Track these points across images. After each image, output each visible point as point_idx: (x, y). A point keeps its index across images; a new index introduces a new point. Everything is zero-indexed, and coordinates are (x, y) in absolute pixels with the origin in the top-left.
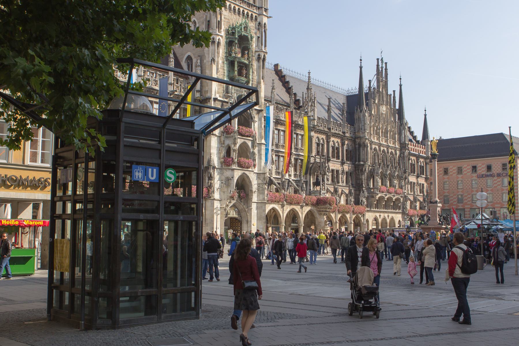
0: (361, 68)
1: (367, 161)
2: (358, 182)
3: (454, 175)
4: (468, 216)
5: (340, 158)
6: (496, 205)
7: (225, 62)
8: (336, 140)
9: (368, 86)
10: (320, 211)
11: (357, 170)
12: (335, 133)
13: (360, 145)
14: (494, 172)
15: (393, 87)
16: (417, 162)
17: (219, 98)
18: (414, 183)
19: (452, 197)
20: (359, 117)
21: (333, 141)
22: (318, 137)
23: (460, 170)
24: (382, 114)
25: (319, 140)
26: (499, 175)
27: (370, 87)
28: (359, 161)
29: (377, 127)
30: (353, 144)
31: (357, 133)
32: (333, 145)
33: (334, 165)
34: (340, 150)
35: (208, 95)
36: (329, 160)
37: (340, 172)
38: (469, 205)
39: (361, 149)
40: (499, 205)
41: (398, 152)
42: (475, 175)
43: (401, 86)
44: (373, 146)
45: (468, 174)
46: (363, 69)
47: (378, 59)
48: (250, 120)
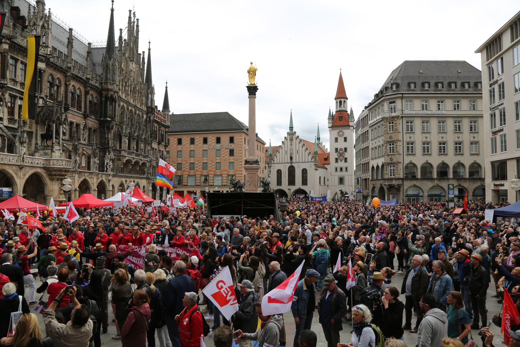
0: (112, 10)
1: (115, 117)
2: (103, 142)
4: (199, 181)
5: (83, 110)
6: (224, 173)
8: (77, 85)
9: (119, 35)
11: (104, 126)
13: (107, 98)
15: (142, 48)
16: (159, 130)
18: (156, 149)
19: (184, 164)
20: (107, 66)
21: (73, 86)
22: (51, 75)
23: (192, 141)
24: (131, 70)
25: (53, 78)
27: (121, 38)
28: (106, 116)
29: (126, 84)
31: (103, 84)
32: (73, 91)
33: (74, 117)
34: (83, 100)
36: (67, 109)
37: (82, 127)
38: (200, 171)
39: (108, 102)
40: (226, 173)
41: (145, 116)
43: (149, 50)
46: (114, 12)
47: (130, 11)
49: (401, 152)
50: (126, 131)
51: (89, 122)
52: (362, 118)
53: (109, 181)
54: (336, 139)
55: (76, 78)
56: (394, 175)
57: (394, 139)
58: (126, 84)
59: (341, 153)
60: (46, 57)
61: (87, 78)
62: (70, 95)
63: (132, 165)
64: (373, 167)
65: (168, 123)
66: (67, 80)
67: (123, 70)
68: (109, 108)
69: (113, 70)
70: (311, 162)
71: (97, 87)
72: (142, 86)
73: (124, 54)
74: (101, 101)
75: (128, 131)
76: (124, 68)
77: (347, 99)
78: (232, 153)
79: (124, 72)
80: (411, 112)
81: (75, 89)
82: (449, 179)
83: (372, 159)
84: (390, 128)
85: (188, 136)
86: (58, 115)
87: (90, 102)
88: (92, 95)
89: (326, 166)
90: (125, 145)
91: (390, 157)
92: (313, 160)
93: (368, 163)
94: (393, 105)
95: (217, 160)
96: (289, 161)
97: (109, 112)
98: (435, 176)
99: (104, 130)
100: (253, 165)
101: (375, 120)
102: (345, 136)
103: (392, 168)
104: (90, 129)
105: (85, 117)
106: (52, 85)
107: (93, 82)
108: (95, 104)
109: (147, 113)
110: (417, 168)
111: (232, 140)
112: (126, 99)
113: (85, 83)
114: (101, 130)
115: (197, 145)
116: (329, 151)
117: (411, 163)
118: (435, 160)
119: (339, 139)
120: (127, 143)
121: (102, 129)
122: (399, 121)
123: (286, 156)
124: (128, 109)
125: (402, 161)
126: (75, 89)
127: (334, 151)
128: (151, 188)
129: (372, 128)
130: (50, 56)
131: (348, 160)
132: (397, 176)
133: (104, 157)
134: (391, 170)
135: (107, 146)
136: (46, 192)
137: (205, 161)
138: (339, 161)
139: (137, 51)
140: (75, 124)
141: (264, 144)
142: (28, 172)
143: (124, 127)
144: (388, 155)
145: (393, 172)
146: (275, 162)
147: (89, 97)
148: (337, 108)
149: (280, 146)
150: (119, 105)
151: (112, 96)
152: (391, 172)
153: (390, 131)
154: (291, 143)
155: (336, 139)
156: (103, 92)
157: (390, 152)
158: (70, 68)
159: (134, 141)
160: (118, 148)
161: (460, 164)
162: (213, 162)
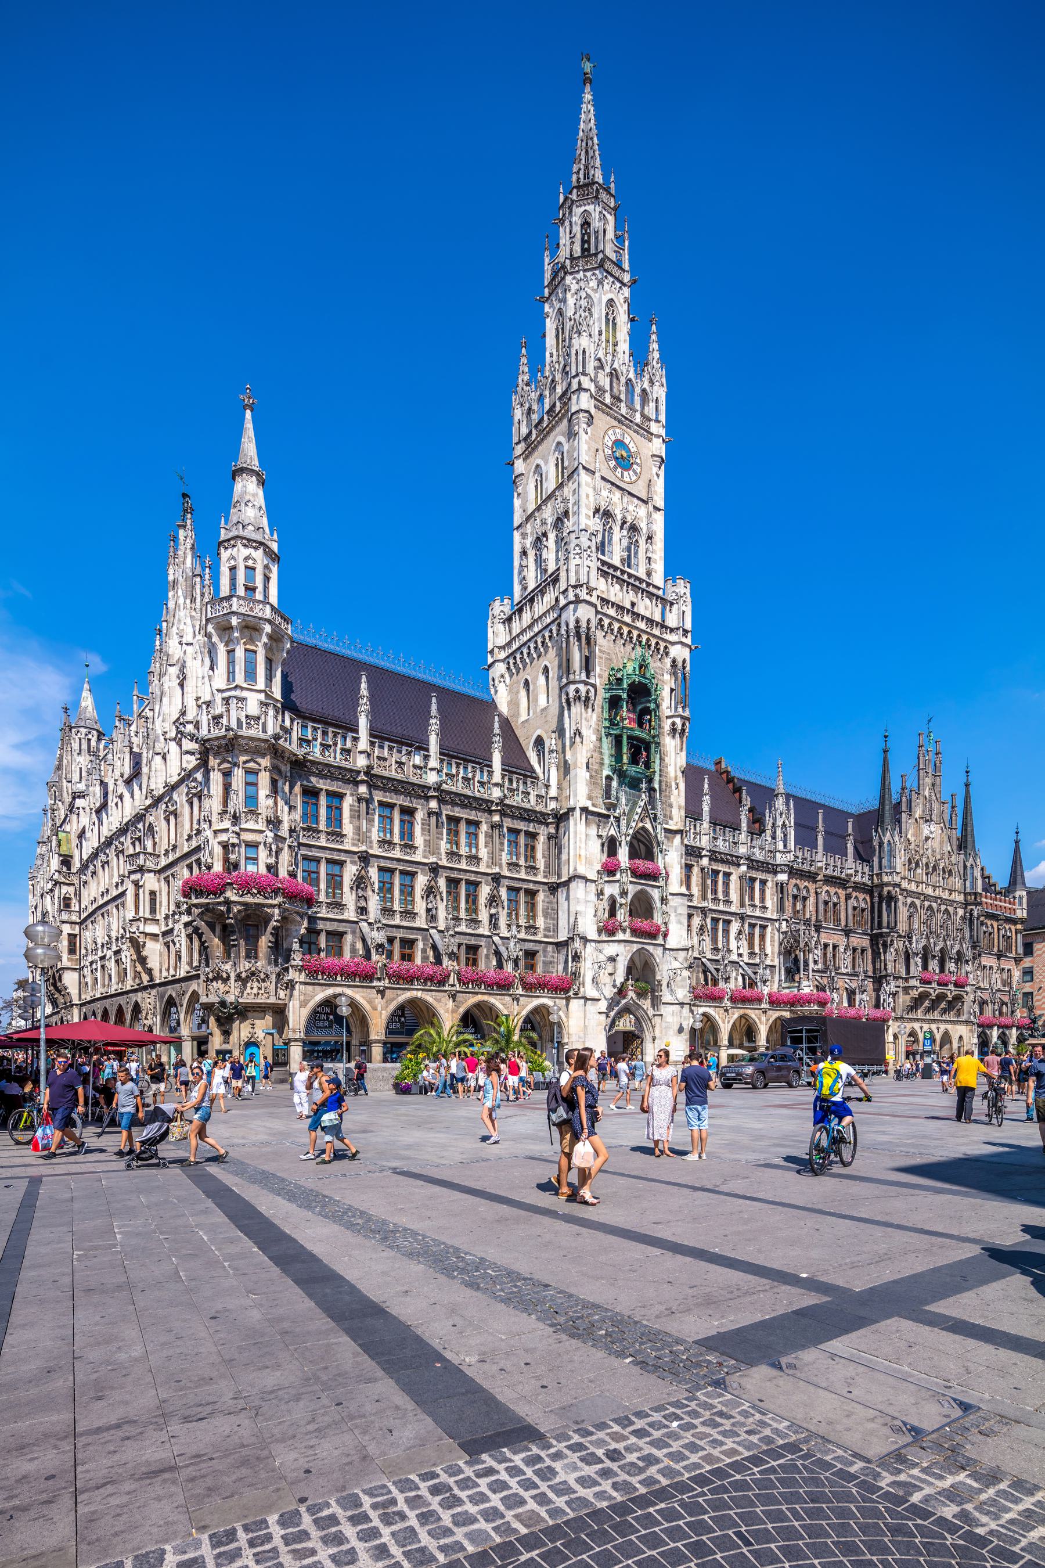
5: (843, 923)
7: (604, 739)
12: (832, 877)
17: (591, 808)
21: (827, 892)
22: (796, 885)
25: (798, 889)
34: (843, 908)
35: (572, 804)
36: (818, 929)
41: (961, 912)
44: (909, 900)
48: (656, 849)
55: (830, 880)
62: (821, 907)
65: (1022, 913)
74: (872, 904)
87: (855, 908)
108: (863, 910)
112: (919, 890)
151: (889, 892)
158: (820, 868)
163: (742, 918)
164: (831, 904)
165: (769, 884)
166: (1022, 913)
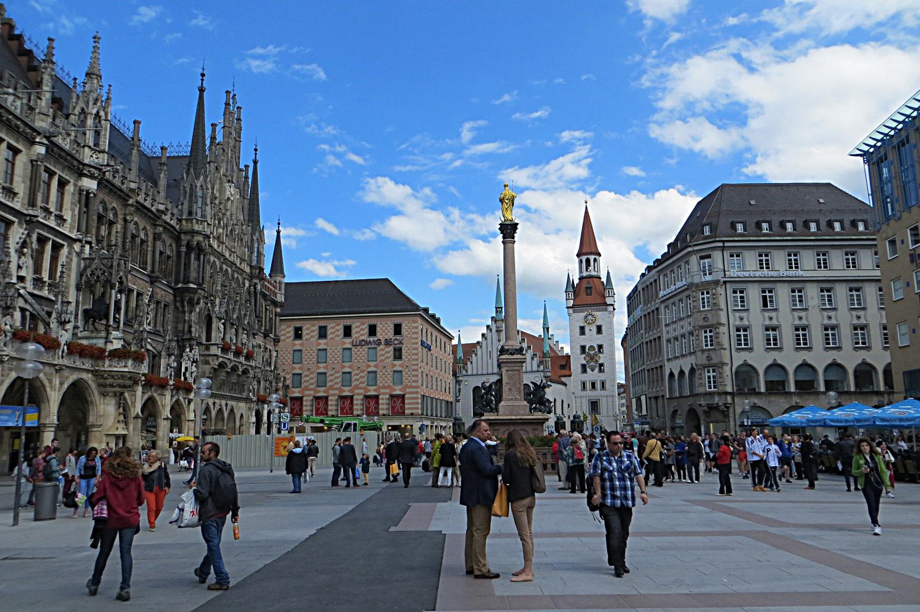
0: (202, 90)
3: (314, 339)
5: (149, 268)
6: (382, 391)
10: (104, 386)
11: (183, 298)
13: (189, 246)
14: (381, 337)
23: (323, 332)
24: (229, 199)
25: (105, 209)
26: (388, 343)
27: (213, 138)
29: (219, 223)
30: (174, 245)
31: (184, 222)
38: (336, 389)
39: (193, 256)
41: (247, 284)
42: (348, 340)
43: (255, 162)
45: (337, 339)
47: (228, 92)
49: (726, 345)
50: (218, 309)
51: (158, 290)
52: (644, 285)
53: (190, 401)
54: (582, 330)
55: (141, 209)
56: (715, 387)
57: (712, 321)
58: (219, 223)
59: (593, 357)
60: (100, 170)
61: (158, 210)
63: (228, 372)
64: (672, 374)
65: (280, 298)
66: (127, 212)
67: (216, 198)
68: (194, 264)
69: (204, 197)
70: (538, 371)
71: (172, 227)
72: (244, 227)
73: (217, 169)
74: (179, 253)
75: (223, 310)
76: (218, 195)
77: (599, 255)
78: (398, 354)
79: (217, 202)
80: (741, 274)
81: (137, 229)
82: (818, 393)
83: (669, 360)
84: (703, 303)
85: (315, 322)
86: (121, 274)
87: (161, 253)
88: (164, 241)
89: (563, 379)
90: (216, 337)
91: (706, 354)
92: (542, 368)
93: (661, 367)
94: (706, 261)
95: (369, 366)
96: (496, 370)
97: (193, 275)
98: (793, 389)
99: (183, 307)
100: (515, 356)
101: (673, 288)
102: (599, 324)
103: (711, 374)
104: (158, 303)
105: (153, 281)
106: (100, 218)
107: (167, 218)
108: (169, 257)
109: (251, 277)
110: (758, 374)
111: (398, 329)
112: (219, 250)
113: (154, 218)
114: (176, 308)
115: (332, 339)
116: (567, 350)
117: (746, 364)
118: (790, 359)
119: (587, 330)
120: (222, 330)
121: (178, 305)
122: (720, 290)
123: (490, 361)
124: (221, 268)
125: (728, 361)
126: (137, 229)
127: (579, 351)
128: (254, 419)
129: (666, 304)
130: (108, 168)
131: (606, 368)
132: (721, 389)
133: (182, 356)
134: (709, 377)
135: (187, 337)
136: (91, 419)
137: (347, 370)
138: (588, 370)
139: (238, 164)
140: (135, 293)
141: (451, 338)
142: (67, 378)
143: (217, 301)
144: (703, 351)
145: (714, 382)
146: (470, 373)
147: (159, 244)
148: (581, 271)
149: (478, 343)
150: (209, 261)
152: (710, 382)
153: (704, 307)
154: (499, 336)
155: (582, 330)
156: (183, 236)
157: (707, 345)
158: (132, 190)
159: (231, 328)
160: (204, 342)
161: (835, 366)
162: (363, 371)
163: (30, 222)
164: (138, 241)
165: (70, 188)
166: (280, 298)
